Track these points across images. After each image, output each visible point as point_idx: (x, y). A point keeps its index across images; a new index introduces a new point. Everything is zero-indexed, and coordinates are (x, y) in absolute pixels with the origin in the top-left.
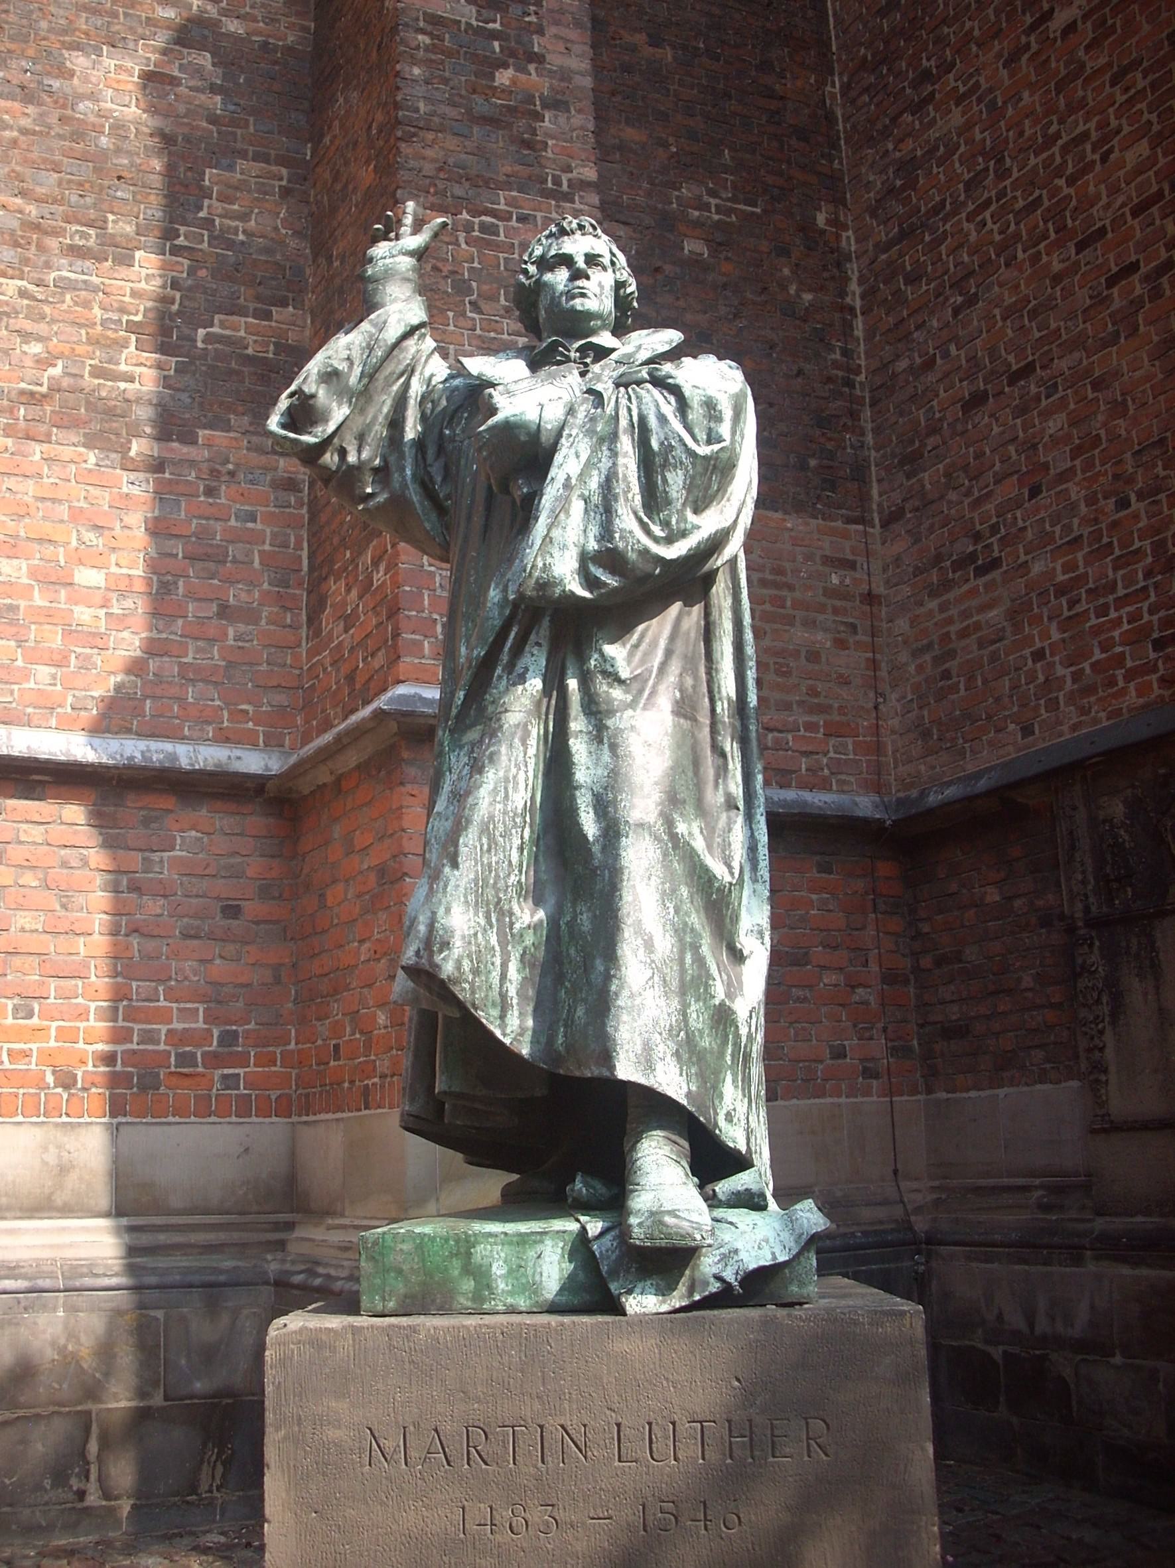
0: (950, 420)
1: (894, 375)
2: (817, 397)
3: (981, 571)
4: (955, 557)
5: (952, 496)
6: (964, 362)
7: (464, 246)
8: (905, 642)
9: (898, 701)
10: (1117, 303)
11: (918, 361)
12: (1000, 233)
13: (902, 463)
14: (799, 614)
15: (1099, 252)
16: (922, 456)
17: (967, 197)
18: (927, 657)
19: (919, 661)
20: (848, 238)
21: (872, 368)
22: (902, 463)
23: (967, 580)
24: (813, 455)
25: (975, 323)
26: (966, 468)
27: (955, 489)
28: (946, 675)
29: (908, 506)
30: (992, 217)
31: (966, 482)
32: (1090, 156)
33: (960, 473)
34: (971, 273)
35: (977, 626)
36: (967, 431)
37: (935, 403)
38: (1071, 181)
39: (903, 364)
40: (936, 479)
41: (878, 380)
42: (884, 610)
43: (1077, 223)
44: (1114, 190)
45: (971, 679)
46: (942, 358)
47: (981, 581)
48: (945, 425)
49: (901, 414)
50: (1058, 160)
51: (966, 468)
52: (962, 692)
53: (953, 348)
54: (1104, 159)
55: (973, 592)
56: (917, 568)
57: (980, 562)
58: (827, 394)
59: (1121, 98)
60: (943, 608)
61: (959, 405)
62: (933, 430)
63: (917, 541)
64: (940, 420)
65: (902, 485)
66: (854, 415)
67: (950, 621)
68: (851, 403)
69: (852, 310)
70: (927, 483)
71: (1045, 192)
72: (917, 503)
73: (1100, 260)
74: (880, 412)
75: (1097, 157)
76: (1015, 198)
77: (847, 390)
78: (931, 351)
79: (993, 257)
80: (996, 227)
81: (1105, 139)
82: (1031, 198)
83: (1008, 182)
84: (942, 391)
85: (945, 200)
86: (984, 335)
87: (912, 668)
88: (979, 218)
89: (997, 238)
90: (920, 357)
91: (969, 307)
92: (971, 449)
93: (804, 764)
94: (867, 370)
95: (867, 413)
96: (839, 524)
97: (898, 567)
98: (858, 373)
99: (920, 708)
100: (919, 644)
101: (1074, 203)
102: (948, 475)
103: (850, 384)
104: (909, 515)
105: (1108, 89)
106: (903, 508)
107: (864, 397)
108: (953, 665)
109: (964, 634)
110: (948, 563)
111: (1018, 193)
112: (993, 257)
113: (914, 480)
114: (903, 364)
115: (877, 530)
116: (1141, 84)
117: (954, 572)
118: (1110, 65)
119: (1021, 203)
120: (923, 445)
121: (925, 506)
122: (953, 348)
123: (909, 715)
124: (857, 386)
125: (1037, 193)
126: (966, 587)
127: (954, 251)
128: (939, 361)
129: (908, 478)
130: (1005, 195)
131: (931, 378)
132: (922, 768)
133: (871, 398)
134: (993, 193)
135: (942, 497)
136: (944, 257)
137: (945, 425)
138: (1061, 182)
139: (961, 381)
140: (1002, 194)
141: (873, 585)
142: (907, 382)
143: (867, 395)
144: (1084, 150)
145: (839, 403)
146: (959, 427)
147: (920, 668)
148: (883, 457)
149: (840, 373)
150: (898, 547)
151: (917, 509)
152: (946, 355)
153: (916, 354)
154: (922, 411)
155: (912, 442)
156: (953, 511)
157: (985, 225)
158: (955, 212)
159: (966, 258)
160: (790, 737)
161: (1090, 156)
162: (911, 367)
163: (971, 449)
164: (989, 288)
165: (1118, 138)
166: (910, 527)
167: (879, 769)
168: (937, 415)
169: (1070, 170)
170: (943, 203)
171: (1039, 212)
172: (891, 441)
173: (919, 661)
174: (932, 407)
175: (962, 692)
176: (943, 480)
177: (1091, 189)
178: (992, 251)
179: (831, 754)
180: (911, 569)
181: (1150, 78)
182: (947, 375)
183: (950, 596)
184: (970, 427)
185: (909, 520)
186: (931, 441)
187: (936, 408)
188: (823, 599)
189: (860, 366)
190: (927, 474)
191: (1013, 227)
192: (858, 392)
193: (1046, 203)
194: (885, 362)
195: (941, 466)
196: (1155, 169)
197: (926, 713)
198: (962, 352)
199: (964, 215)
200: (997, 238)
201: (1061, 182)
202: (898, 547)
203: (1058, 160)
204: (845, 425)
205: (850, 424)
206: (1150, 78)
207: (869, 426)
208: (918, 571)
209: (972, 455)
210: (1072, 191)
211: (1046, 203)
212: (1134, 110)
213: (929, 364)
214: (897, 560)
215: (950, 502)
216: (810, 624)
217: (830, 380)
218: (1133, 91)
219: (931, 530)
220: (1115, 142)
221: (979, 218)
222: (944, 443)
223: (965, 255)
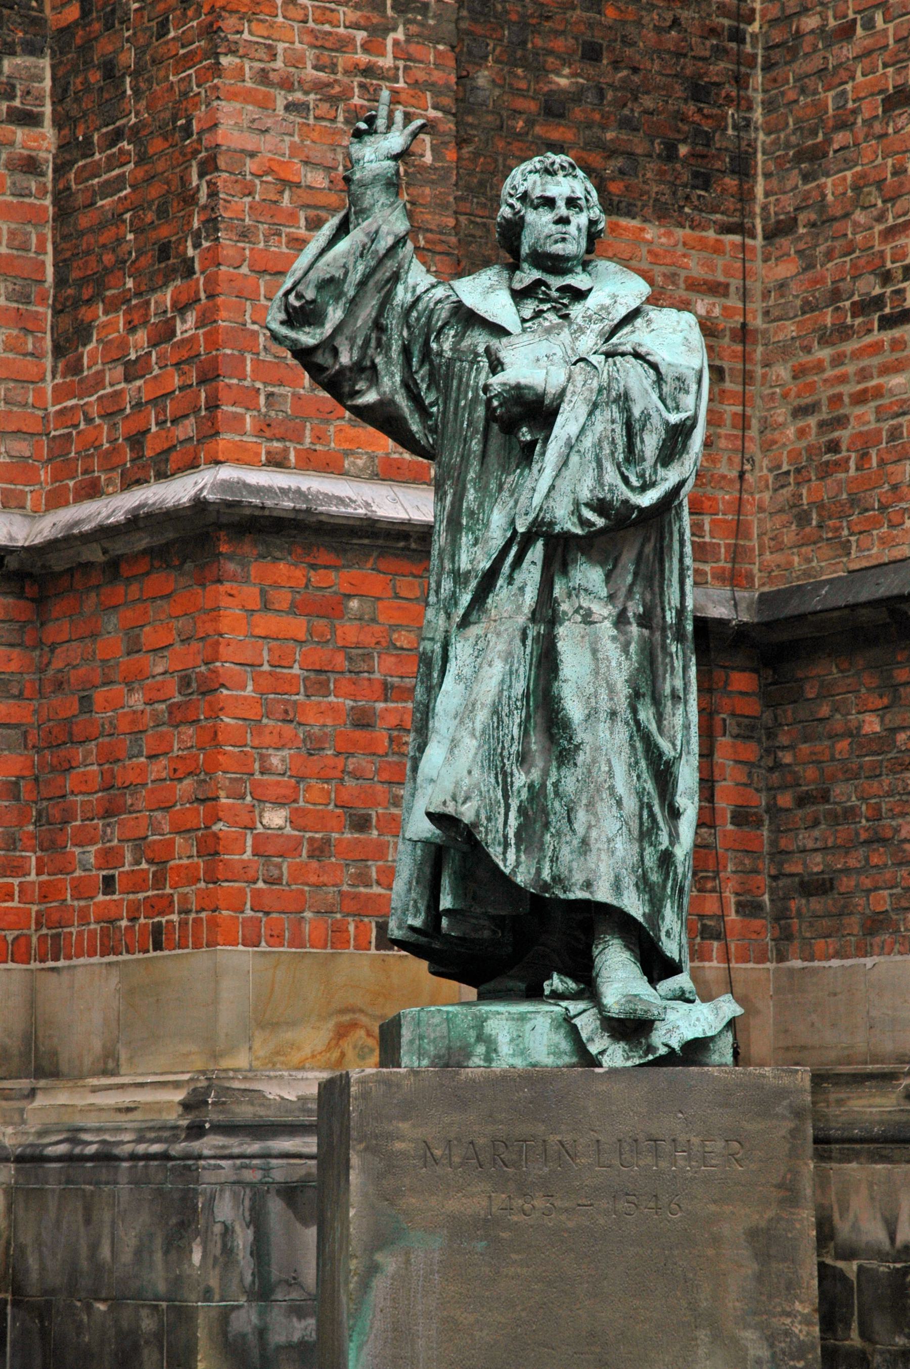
0: (867, 115)
1: (798, 35)
2: (694, 57)
3: (887, 323)
4: (856, 298)
5: (860, 216)
6: (891, 41)
9: (770, 470)
11: (832, 23)
13: (800, 157)
16: (825, 155)
19: (801, 424)
21: (769, 17)
22: (800, 157)
23: (870, 331)
26: (880, 184)
27: (864, 208)
29: (802, 217)
31: (880, 203)
33: (873, 189)
35: (878, 392)
36: (886, 135)
37: (849, 87)
39: (811, 22)
40: (841, 189)
41: (777, 36)
42: (760, 349)
46: (864, 28)
47: (887, 336)
48: (859, 120)
49: (803, 91)
51: (880, 184)
55: (876, 348)
56: (806, 302)
57: (887, 310)
58: (707, 54)
60: (838, 360)
61: (880, 98)
62: (843, 125)
63: (810, 266)
64: (855, 112)
65: (796, 187)
66: (740, 81)
68: (739, 63)
70: (828, 191)
72: (813, 217)
74: (775, 80)
77: (733, 45)
78: (851, 15)
84: (859, 73)
90: (835, 18)
92: (890, 161)
94: (763, 16)
95: (758, 79)
97: (782, 296)
98: (751, 21)
102: (857, 188)
103: (738, 36)
104: (802, 231)
106: (795, 220)
107: (754, 56)
113: (814, 184)
114: (811, 22)
117: (853, 317)
120: (828, 141)
121: (824, 222)
123: (784, 491)
124: (748, 39)
128: (859, 31)
129: (807, 177)
131: (848, 51)
133: (766, 58)
135: (847, 215)
137: (859, 120)
139: (885, 65)
141: (750, 317)
142: (815, 49)
143: (760, 52)
145: (722, 65)
146: (878, 128)
148: (773, 143)
149: (726, 22)
150: (785, 270)
151: (814, 225)
152: (869, 24)
153: (830, 13)
154: (831, 94)
155: (814, 133)
156: (859, 237)
162: (822, 28)
163: (890, 161)
166: (802, 246)
168: (850, 105)
172: (787, 124)
173: (801, 424)
174: (844, 92)
176: (850, 193)
182: (868, 53)
184: (891, 130)
185: (800, 238)
186: (841, 138)
187: (850, 95)
189: (753, 11)
190: (829, 181)
192: (748, 48)
194: (789, 11)
195: (848, 174)
198: (891, 26)
202: (785, 270)
204: (728, 96)
205: (734, 94)
207: (759, 97)
208: (808, 307)
209: (889, 169)
213: (846, 32)
214: (782, 286)
215: (856, 224)
217: (713, 32)
219: (829, 255)
222: (856, 145)
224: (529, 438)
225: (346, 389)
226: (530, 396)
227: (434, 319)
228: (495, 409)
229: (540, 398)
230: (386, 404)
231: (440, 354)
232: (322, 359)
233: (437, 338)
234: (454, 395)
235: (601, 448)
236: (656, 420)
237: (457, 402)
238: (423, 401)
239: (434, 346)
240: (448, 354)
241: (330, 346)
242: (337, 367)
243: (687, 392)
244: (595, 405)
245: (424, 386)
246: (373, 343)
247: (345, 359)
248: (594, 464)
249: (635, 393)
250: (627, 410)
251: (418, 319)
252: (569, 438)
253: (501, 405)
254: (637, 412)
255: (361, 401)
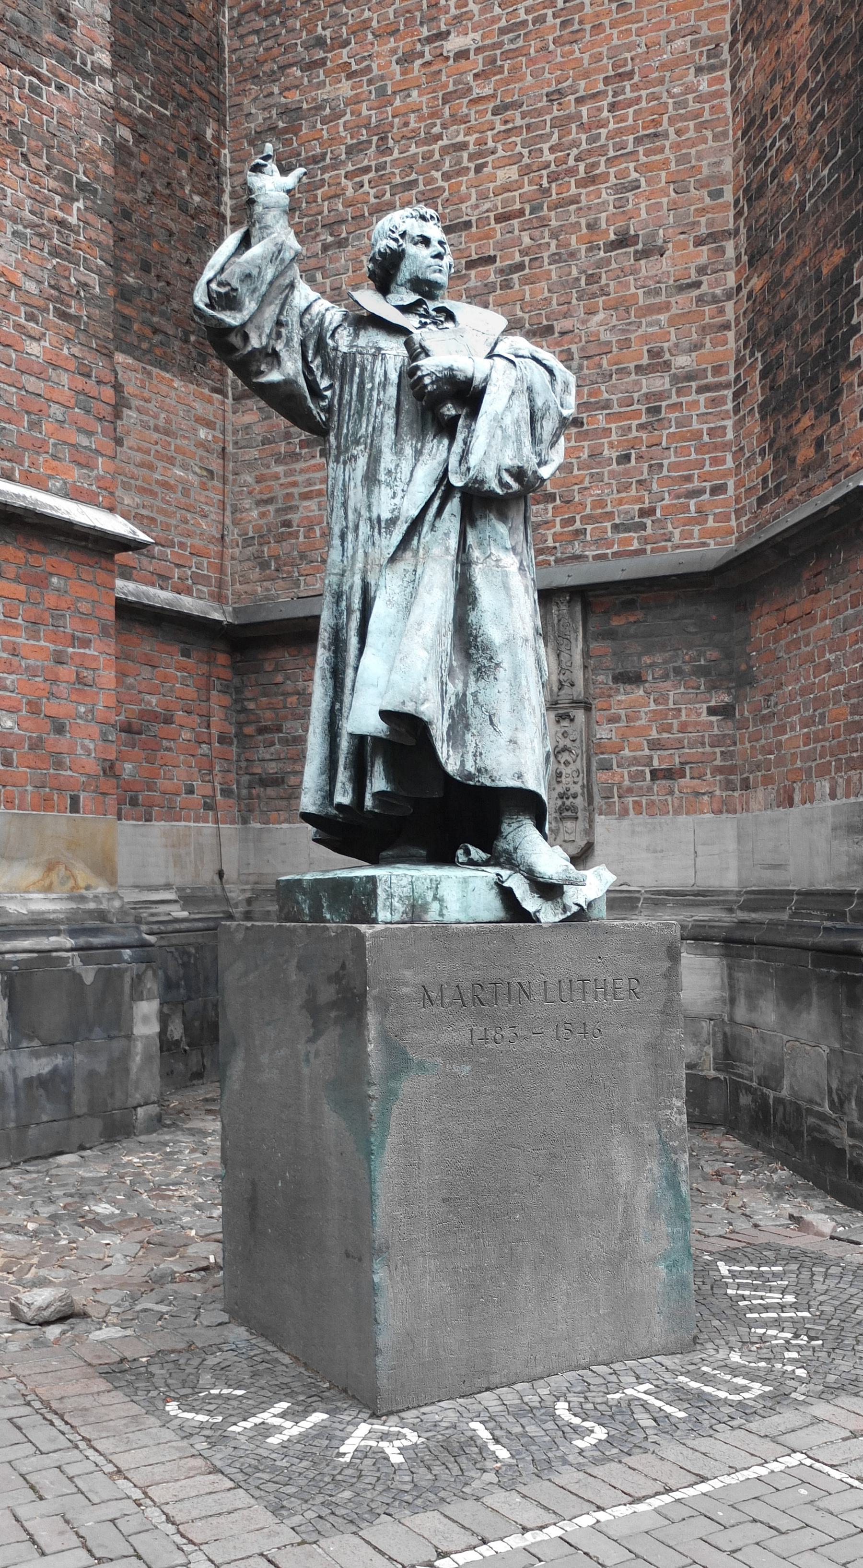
7: (17, 100)
8: (250, 493)
10: (472, 283)
12: (376, 197)
14: (179, 457)
15: (463, 239)
17: (348, 158)
18: (271, 508)
20: (225, 155)
24: (193, 333)
25: (343, 261)
28: (287, 524)
30: (370, 182)
32: (465, 163)
34: (344, 221)
38: (446, 177)
43: (447, 211)
44: (483, 196)
45: (310, 529)
50: (437, 157)
52: (301, 539)
53: (319, 276)
54: (479, 169)
59: (500, 127)
67: (295, 484)
69: (224, 217)
71: (421, 177)
73: (463, 246)
75: (472, 166)
76: (393, 173)
79: (367, 214)
80: (372, 192)
81: (480, 154)
82: (407, 179)
83: (388, 159)
85: (326, 153)
86: (350, 273)
87: (255, 514)
88: (357, 179)
89: (373, 200)
91: (339, 247)
93: (176, 573)
96: (206, 391)
99: (261, 544)
100: (265, 497)
101: (447, 193)
105: (489, 116)
108: (295, 517)
109: (306, 496)
110: (297, 441)
111: (397, 171)
112: (367, 214)
115: (230, 401)
116: (519, 122)
118: (494, 96)
119: (398, 180)
122: (319, 276)
125: (413, 176)
126: (313, 462)
127: (331, 198)
130: (384, 168)
132: (259, 589)
134: (373, 163)
136: (319, 200)
138: (438, 175)
140: (380, 167)
144: (462, 157)
147: (263, 515)
157: (362, 186)
158: (334, 167)
159: (340, 207)
160: (169, 551)
161: (465, 163)
164: (359, 238)
165: (493, 157)
167: (221, 584)
169: (446, 167)
170: (323, 156)
171: (414, 192)
175: (301, 539)
177: (463, 188)
178: (366, 209)
179: (194, 569)
180: (260, 438)
181: (527, 120)
183: (298, 466)
188: (193, 448)
191: (388, 195)
193: (421, 187)
196: (520, 191)
197: (266, 549)
199: (343, 172)
200: (373, 200)
201: (438, 175)
203: (437, 157)
206: (527, 120)
210: (446, 185)
211: (421, 187)
212: (510, 140)
216: (184, 467)
218: (510, 126)
220: (489, 159)
221: (357, 179)
223: (340, 205)
224: (453, 412)
225: (254, 368)
226: (460, 376)
227: (326, 324)
228: (426, 386)
229: (469, 381)
230: (289, 383)
231: (336, 349)
232: (235, 340)
233: (332, 336)
234: (356, 379)
235: (519, 426)
236: (553, 412)
237: (362, 384)
238: (318, 385)
239: (330, 342)
240: (344, 349)
241: (242, 331)
242: (250, 349)
243: (570, 394)
244: (513, 393)
245: (318, 374)
246: (274, 336)
247: (255, 342)
248: (514, 438)
249: (538, 387)
250: (531, 400)
251: (311, 321)
252: (497, 414)
253: (432, 383)
254: (539, 403)
255: (264, 379)
